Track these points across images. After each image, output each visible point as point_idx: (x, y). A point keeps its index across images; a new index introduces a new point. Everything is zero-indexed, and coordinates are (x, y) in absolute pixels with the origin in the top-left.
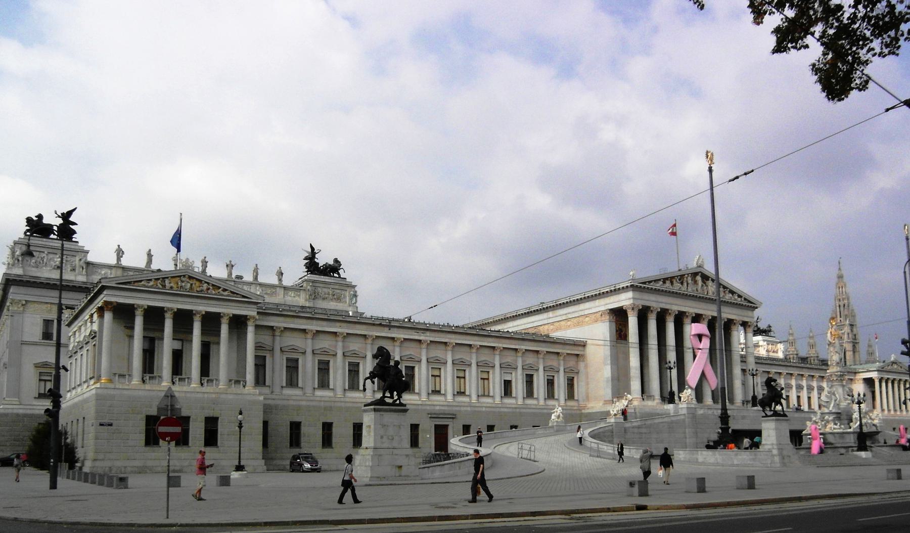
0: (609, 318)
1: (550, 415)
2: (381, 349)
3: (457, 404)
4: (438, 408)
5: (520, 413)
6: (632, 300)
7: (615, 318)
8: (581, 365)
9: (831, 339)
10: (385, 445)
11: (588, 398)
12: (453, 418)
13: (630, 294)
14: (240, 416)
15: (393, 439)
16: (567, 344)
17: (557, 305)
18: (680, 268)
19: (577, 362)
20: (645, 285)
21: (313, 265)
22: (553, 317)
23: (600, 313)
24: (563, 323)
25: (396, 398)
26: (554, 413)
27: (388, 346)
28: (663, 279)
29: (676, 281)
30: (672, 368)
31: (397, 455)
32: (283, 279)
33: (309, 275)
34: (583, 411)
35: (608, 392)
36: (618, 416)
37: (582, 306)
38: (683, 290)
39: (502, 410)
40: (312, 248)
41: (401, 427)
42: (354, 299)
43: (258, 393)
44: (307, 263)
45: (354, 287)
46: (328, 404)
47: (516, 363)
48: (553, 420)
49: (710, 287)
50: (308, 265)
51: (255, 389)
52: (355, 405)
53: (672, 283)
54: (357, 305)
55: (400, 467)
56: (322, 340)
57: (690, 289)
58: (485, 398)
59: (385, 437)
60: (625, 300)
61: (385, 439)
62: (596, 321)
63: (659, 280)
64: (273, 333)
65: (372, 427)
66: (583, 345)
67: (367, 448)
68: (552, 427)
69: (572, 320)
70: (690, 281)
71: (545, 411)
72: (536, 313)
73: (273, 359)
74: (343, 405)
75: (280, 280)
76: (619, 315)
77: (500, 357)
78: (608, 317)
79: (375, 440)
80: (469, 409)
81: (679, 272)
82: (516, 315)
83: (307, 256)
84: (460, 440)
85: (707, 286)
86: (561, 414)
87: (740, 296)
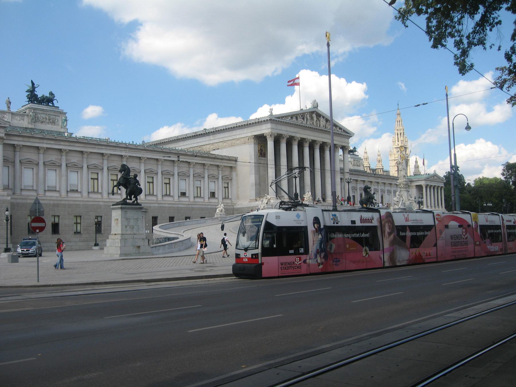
0: (254, 141)
1: (216, 209)
2: (123, 166)
3: (148, 202)
5: (192, 208)
6: (270, 129)
7: (258, 141)
8: (234, 174)
9: (401, 160)
10: (128, 232)
11: (238, 198)
14: (7, 213)
15: (134, 227)
17: (216, 131)
18: (301, 108)
19: (231, 171)
20: (279, 120)
21: (33, 96)
22: (213, 140)
23: (248, 138)
24: (220, 144)
25: (134, 199)
26: (218, 208)
27: (132, 165)
29: (300, 117)
30: (297, 177)
31: (136, 239)
32: (12, 106)
33: (31, 104)
34: (235, 207)
35: (252, 193)
37: (234, 133)
38: (304, 123)
39: (180, 206)
40: (33, 84)
41: (139, 219)
42: (65, 123)
43: (6, 194)
44: (29, 94)
45: (65, 113)
46: (56, 202)
47: (189, 172)
48: (218, 213)
49: (321, 122)
50: (29, 96)
51: (4, 191)
52: (76, 203)
53: (297, 118)
54: (67, 127)
55: (139, 247)
56: (50, 154)
57: (308, 123)
58: (167, 197)
59: (128, 227)
60: (265, 130)
61: (128, 228)
62: (245, 143)
63: (289, 116)
64: (38, 152)
65: (120, 220)
67: (115, 234)
68: (217, 218)
69: (227, 142)
70: (308, 118)
71: (209, 207)
72: (201, 136)
73: (14, 169)
74: (67, 203)
75: (9, 107)
76: (261, 140)
77: (178, 168)
78: (253, 141)
79: (122, 230)
80: (156, 205)
81: (301, 111)
82: (186, 137)
83: (29, 90)
84: (159, 227)
85: (319, 121)
86: (223, 209)
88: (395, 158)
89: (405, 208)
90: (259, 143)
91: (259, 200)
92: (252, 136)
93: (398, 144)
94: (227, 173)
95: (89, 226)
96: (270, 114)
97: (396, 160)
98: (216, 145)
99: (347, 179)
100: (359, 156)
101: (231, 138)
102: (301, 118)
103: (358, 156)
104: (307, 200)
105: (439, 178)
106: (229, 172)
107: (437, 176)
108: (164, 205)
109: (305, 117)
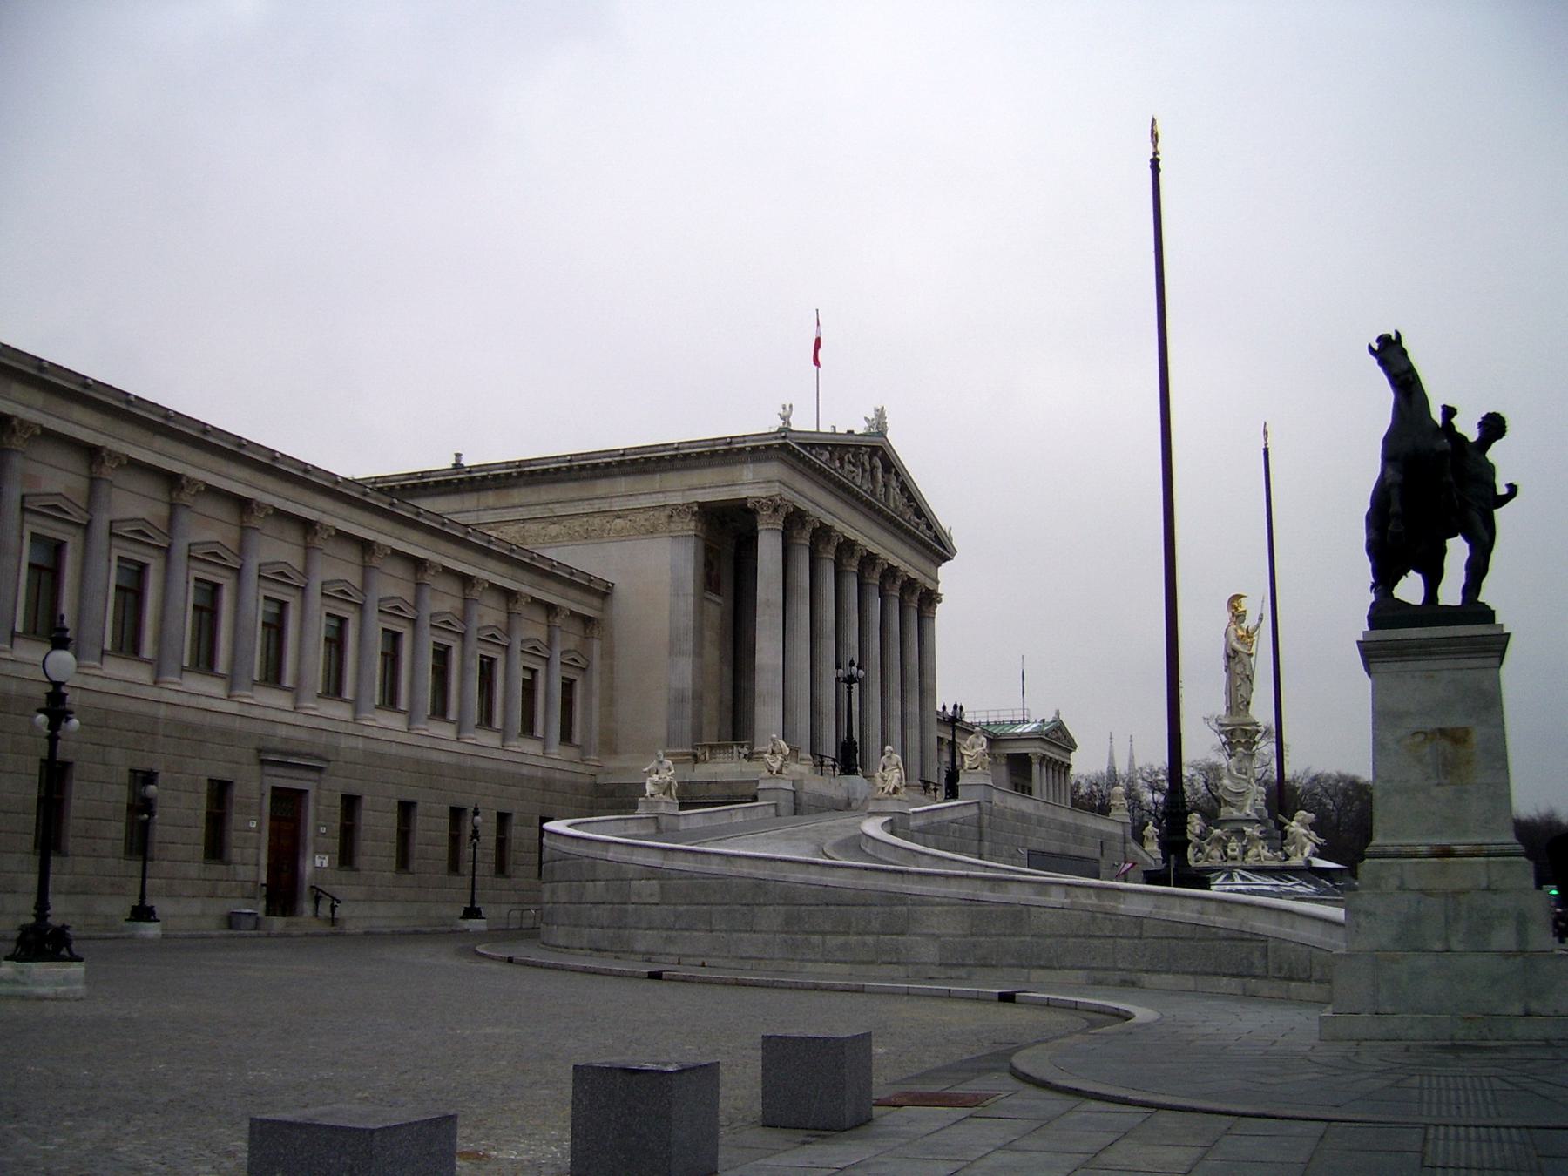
4: (283, 731)
7: (704, 527)
8: (596, 646)
12: (319, 770)
13: (773, 470)
16: (573, 584)
19: (586, 637)
23: (668, 512)
26: (649, 773)
29: (849, 458)
36: (899, 796)
37: (602, 487)
39: (434, 756)
48: (652, 796)
49: (892, 490)
53: (842, 466)
62: (652, 532)
66: (602, 592)
71: (525, 770)
78: (692, 525)
80: (360, 744)
87: (929, 526)
89: (1257, 818)
91: (711, 758)
92: (689, 505)
94: (568, 639)
95: (100, 819)
96: (780, 423)
98: (516, 528)
101: (585, 508)
104: (975, 766)
106: (577, 638)
108: (386, 748)
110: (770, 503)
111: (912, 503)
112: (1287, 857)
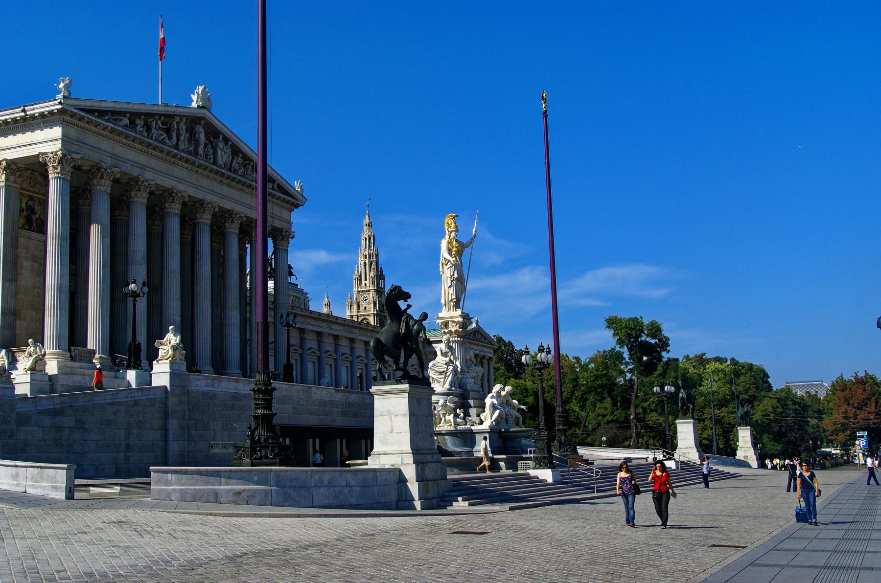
0: (7, 180)
13: (57, 132)
28: (131, 113)
29: (157, 124)
30: (139, 295)
49: (219, 151)
57: (182, 147)
63: (123, 113)
88: (357, 312)
90: (22, 189)
93: (365, 284)
97: (361, 316)
99: (285, 316)
100: (299, 287)
102: (159, 127)
103: (297, 285)
105: (485, 338)
107: (480, 334)
109: (173, 129)
110: (55, 156)
111: (247, 162)
112: (481, 423)
